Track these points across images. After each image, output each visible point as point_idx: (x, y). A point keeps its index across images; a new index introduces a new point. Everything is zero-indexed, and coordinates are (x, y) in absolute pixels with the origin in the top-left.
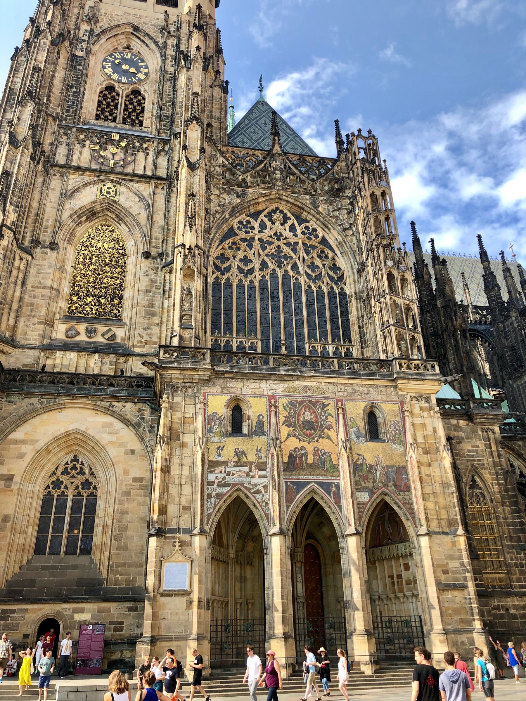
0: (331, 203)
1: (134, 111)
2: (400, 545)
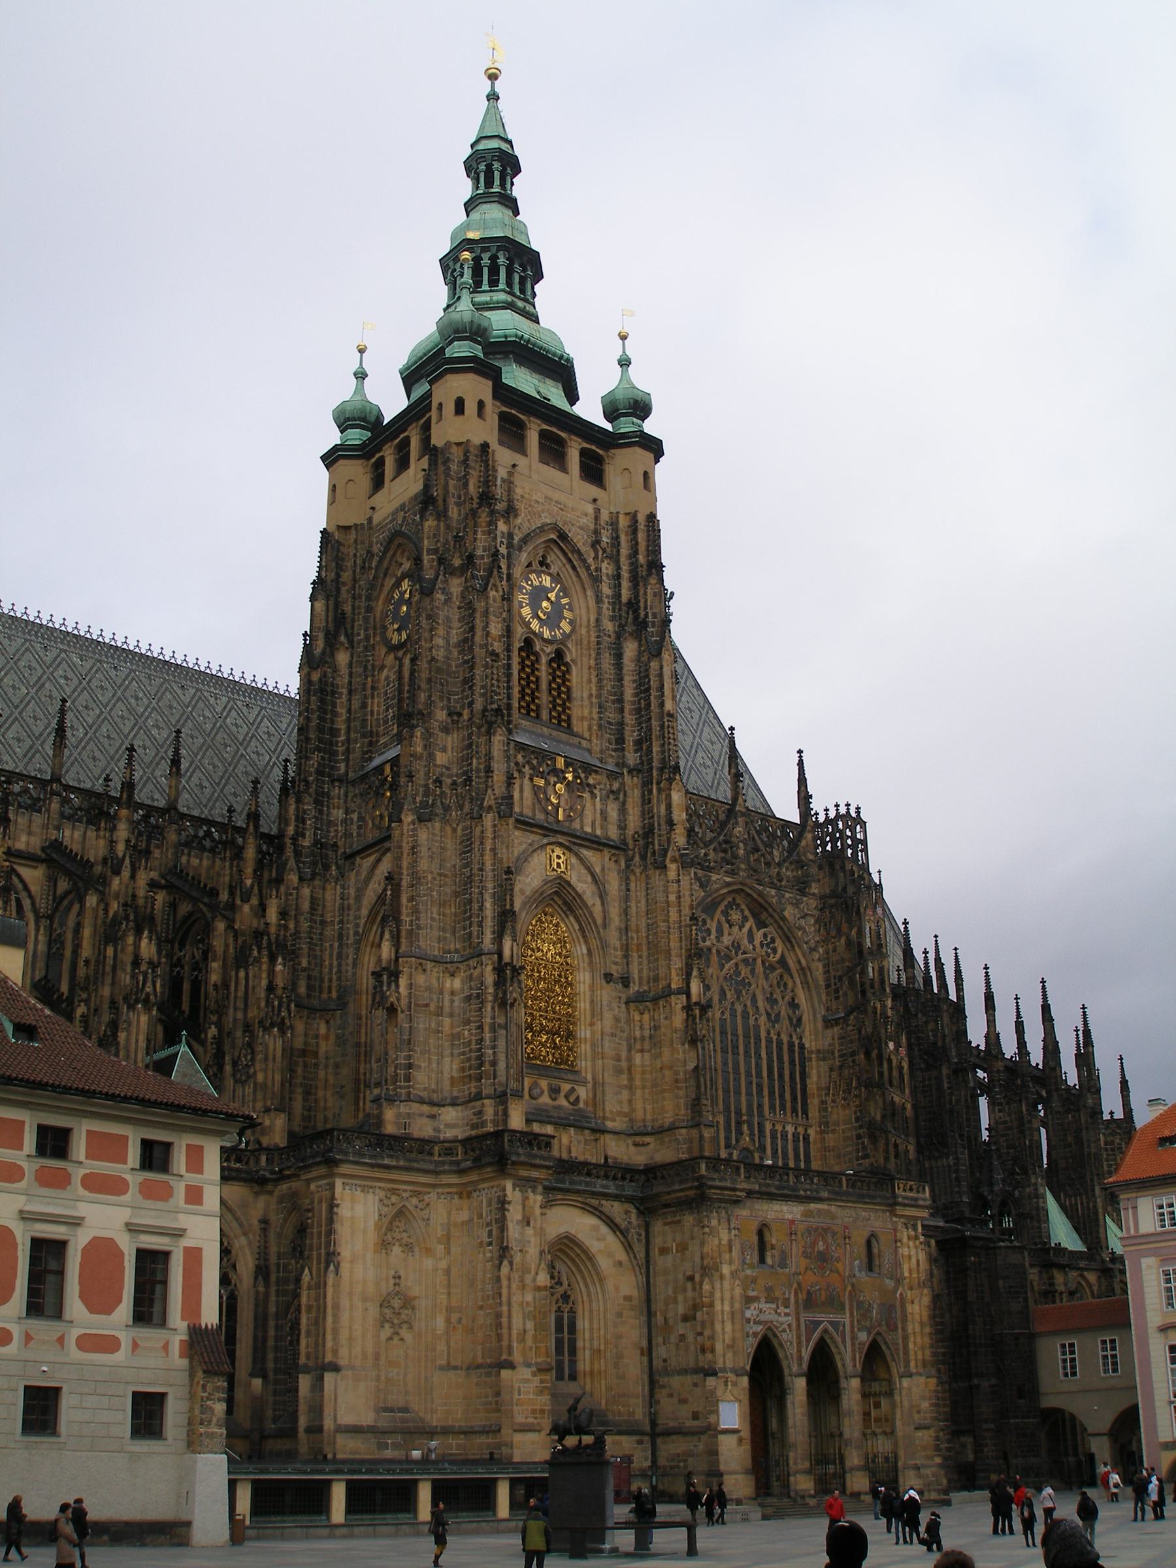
0: (796, 905)
1: (559, 695)
2: (873, 1384)
